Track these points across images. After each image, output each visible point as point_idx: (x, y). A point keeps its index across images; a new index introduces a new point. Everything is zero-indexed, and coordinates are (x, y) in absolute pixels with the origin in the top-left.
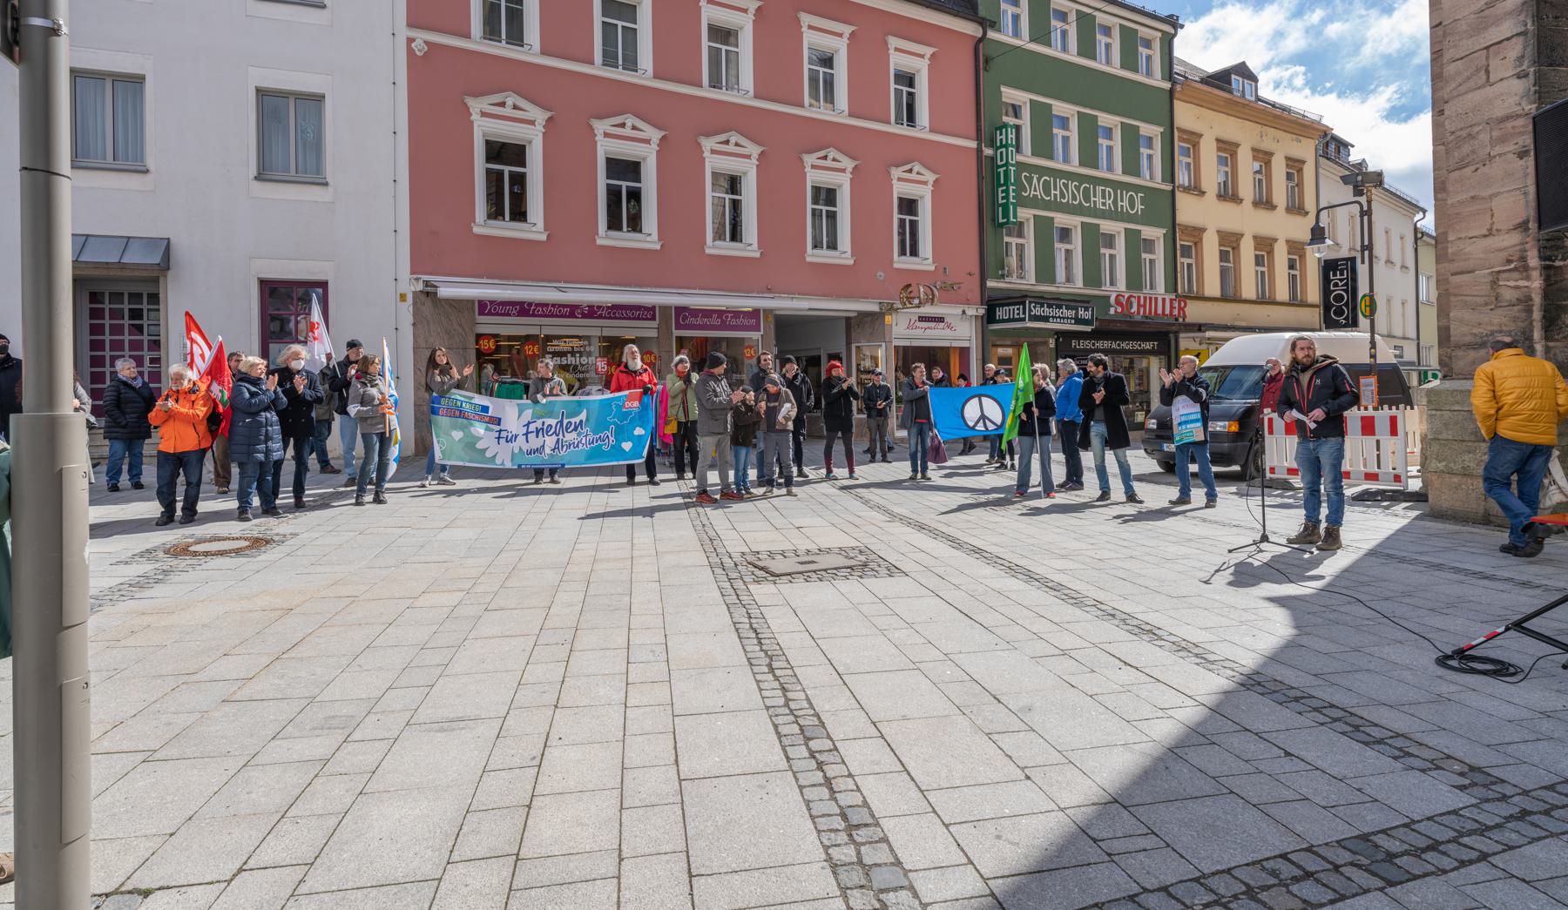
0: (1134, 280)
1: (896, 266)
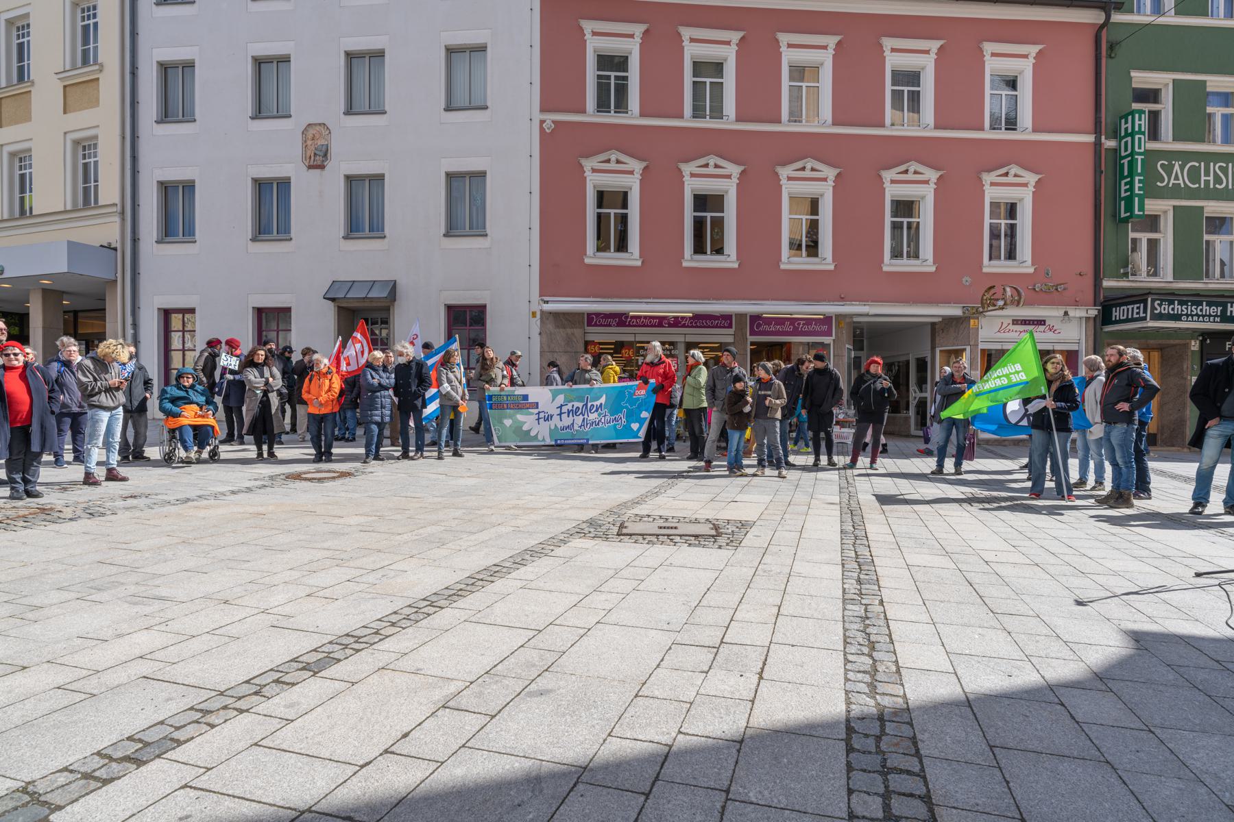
1: (985, 270)
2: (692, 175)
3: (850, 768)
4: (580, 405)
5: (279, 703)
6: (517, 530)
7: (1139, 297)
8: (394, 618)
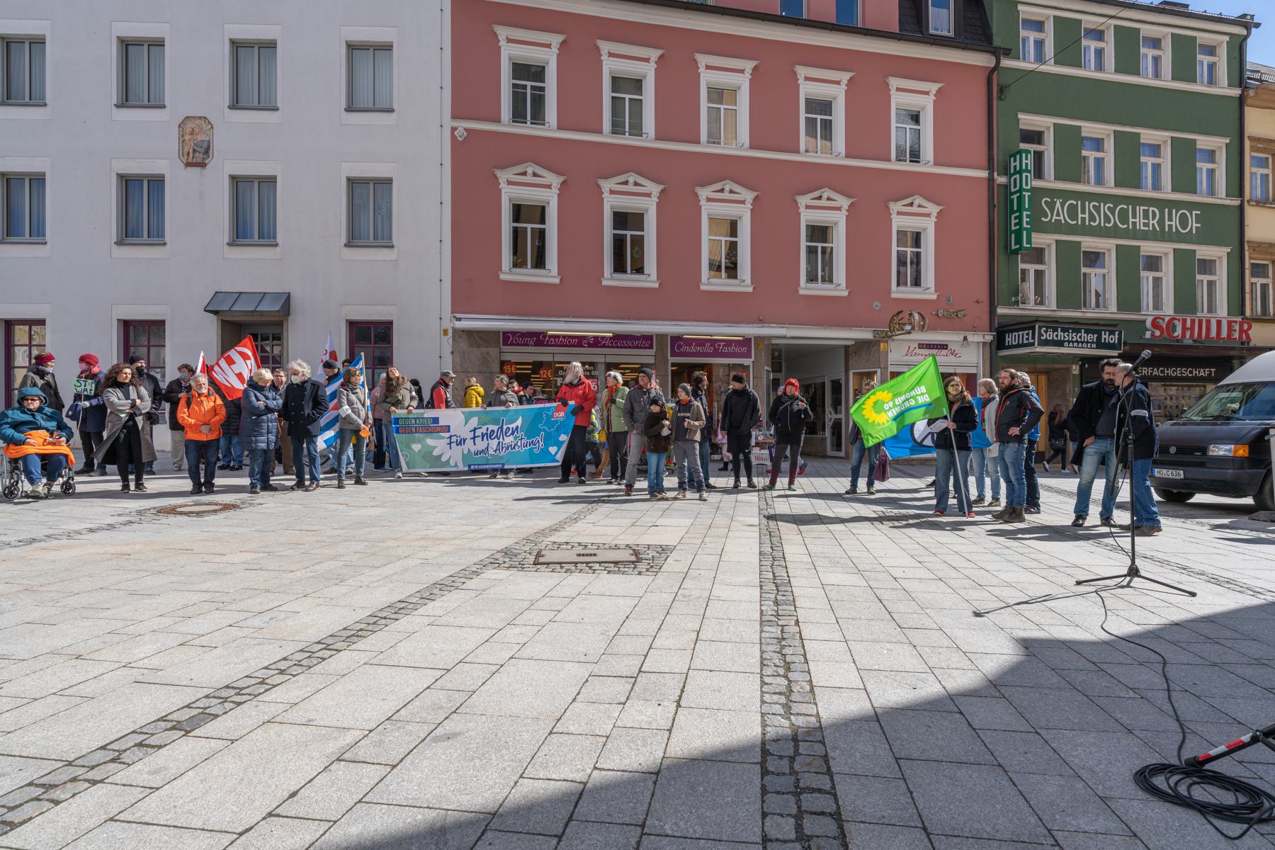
0: (1186, 300)
1: (893, 296)
2: (612, 192)
3: (764, 791)
4: (495, 428)
5: (141, 770)
6: (426, 563)
7: (1028, 324)
8: (283, 665)
